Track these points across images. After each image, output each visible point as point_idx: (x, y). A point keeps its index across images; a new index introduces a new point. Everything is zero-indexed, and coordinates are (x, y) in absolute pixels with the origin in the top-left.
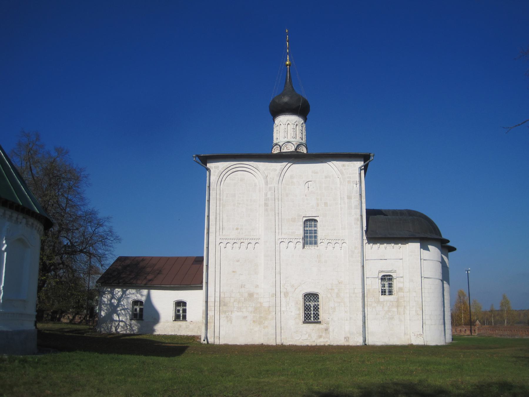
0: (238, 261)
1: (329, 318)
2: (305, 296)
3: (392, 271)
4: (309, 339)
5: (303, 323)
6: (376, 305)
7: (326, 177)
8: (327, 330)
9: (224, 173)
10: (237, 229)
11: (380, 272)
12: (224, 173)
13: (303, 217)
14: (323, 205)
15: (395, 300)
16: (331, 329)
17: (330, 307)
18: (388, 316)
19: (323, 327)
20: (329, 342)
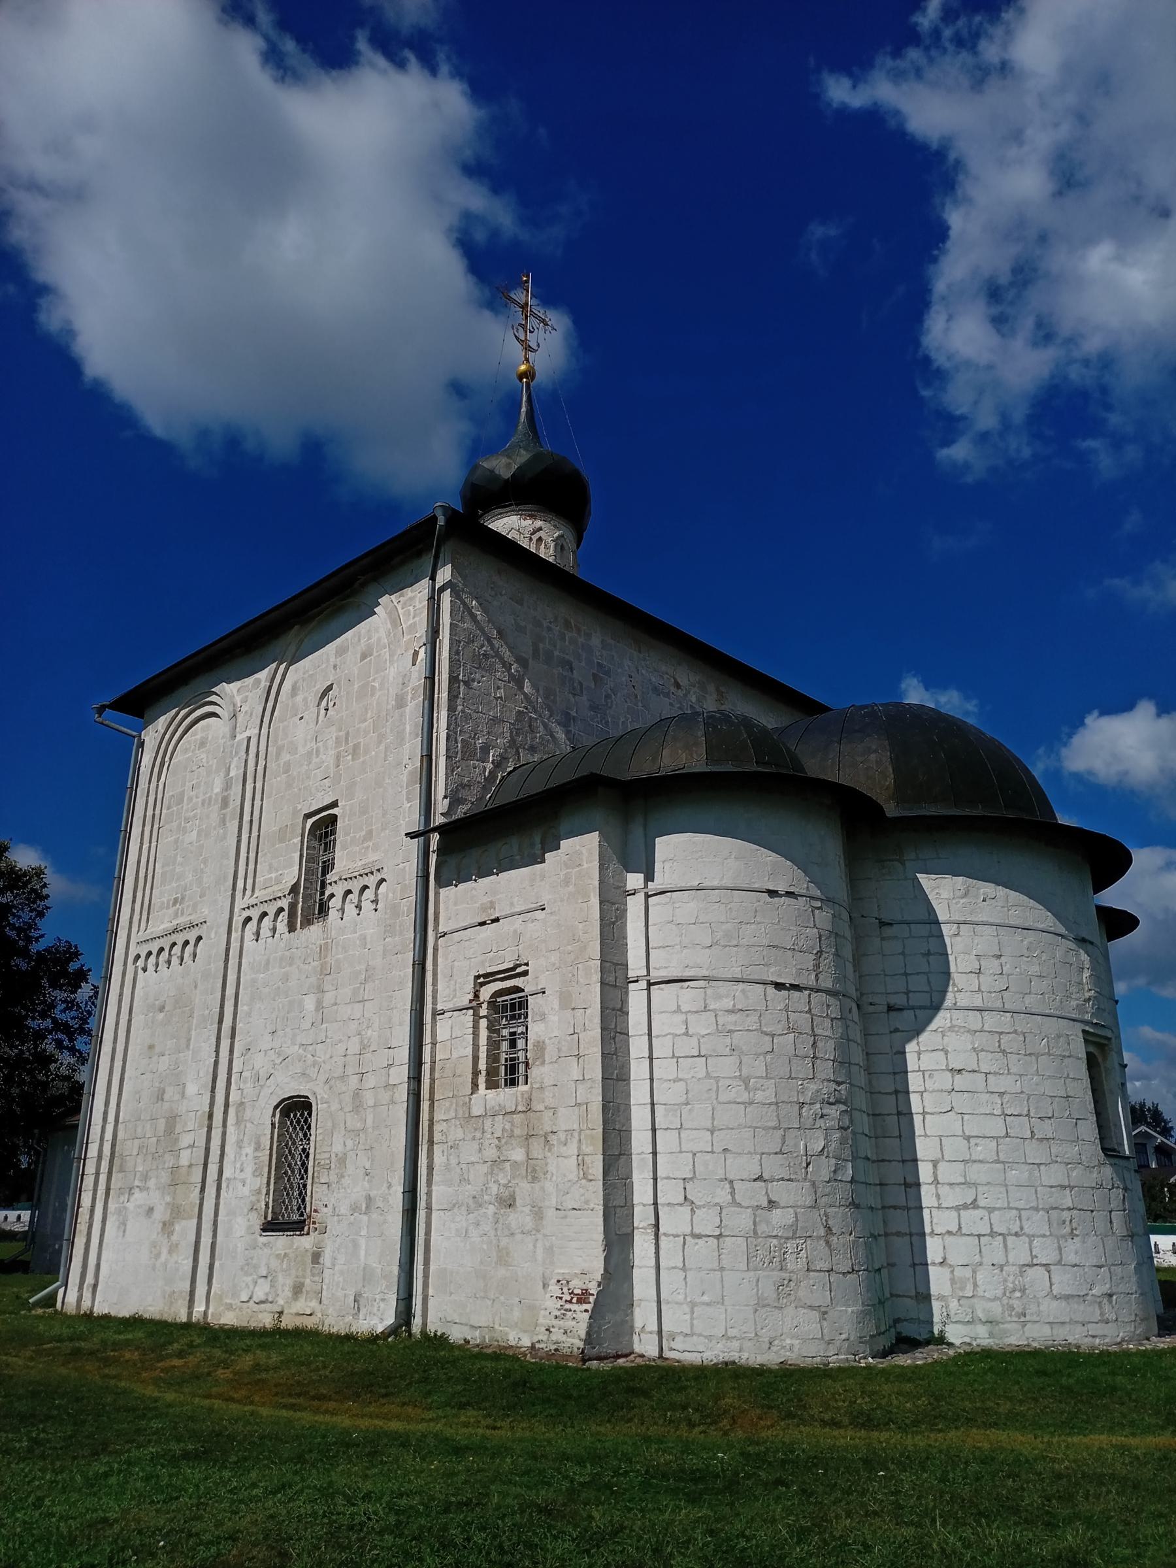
0: (162, 1009)
1: (326, 1206)
2: (285, 1113)
3: (519, 970)
4: (270, 1300)
5: (264, 1230)
6: (459, 1134)
7: (364, 656)
8: (316, 1257)
9: (167, 737)
10: (176, 901)
11: (482, 980)
12: (167, 737)
13: (308, 816)
14: (350, 757)
15: (520, 1108)
16: (326, 1259)
17: (333, 1156)
18: (494, 1189)
19: (308, 1246)
20: (319, 1315)
